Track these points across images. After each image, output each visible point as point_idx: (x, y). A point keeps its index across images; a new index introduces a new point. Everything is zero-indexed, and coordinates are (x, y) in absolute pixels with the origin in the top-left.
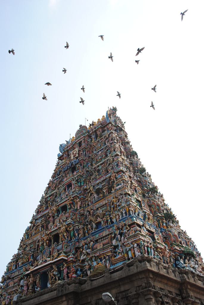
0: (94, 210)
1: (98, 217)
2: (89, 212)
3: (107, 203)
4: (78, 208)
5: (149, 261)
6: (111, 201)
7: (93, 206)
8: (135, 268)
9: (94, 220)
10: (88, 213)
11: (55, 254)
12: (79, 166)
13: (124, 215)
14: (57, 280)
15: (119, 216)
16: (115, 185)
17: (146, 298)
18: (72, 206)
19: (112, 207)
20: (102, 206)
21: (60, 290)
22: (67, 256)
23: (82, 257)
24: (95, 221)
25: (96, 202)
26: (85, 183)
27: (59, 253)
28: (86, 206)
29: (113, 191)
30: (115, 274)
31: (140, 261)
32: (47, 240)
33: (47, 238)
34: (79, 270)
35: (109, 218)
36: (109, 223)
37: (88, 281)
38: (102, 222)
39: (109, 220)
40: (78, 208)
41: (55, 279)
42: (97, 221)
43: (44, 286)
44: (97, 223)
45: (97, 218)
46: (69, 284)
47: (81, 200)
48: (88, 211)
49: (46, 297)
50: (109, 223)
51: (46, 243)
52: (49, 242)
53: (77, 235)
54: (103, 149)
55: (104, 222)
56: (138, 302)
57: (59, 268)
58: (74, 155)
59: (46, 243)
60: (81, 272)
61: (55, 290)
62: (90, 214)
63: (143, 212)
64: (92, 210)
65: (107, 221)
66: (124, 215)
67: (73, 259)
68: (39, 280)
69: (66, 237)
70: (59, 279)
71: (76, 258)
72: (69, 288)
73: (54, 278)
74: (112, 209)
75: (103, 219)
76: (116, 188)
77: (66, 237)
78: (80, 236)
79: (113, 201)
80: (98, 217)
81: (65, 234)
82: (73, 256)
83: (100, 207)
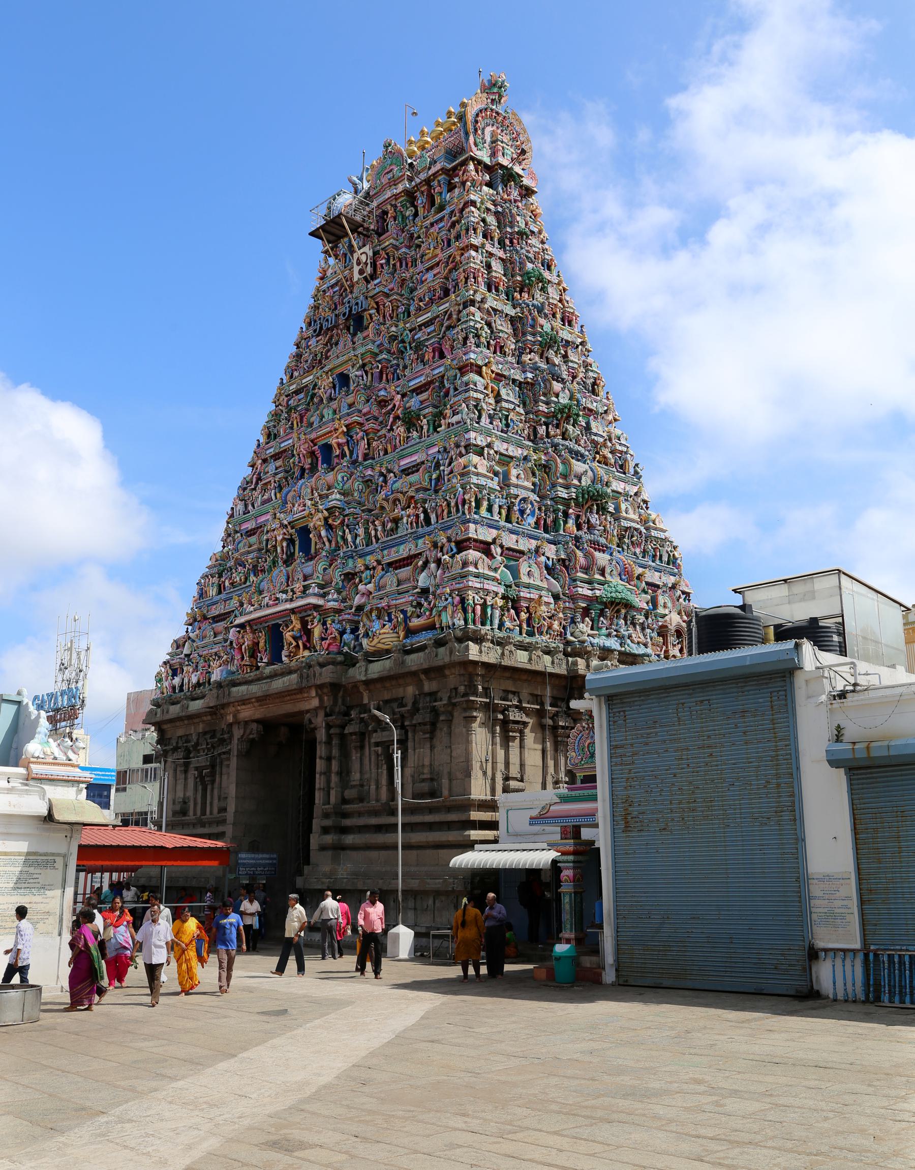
4: (360, 459)
5: (479, 639)
6: (435, 458)
8: (448, 653)
11: (298, 586)
12: (370, 315)
13: (453, 510)
14: (301, 650)
15: (443, 511)
16: (447, 411)
17: (467, 714)
21: (305, 675)
22: (324, 596)
23: (358, 600)
26: (384, 376)
27: (306, 583)
29: (443, 427)
30: (413, 656)
31: (460, 640)
32: (284, 539)
33: (285, 534)
34: (348, 631)
37: (361, 664)
39: (422, 516)
40: (360, 459)
41: (297, 646)
43: (276, 658)
46: (322, 665)
47: (367, 435)
48: (382, 474)
49: (279, 684)
51: (282, 547)
52: (288, 546)
53: (349, 538)
54: (437, 264)
56: (451, 721)
57: (304, 623)
58: (360, 267)
59: (282, 547)
60: (352, 636)
61: (295, 671)
63: (509, 496)
65: (417, 516)
66: (453, 510)
67: (336, 603)
68: (266, 642)
69: (325, 539)
70: (305, 648)
71: (344, 600)
72: (320, 674)
73: (294, 644)
76: (450, 421)
77: (325, 539)
78: (358, 541)
81: (323, 533)
82: (335, 596)
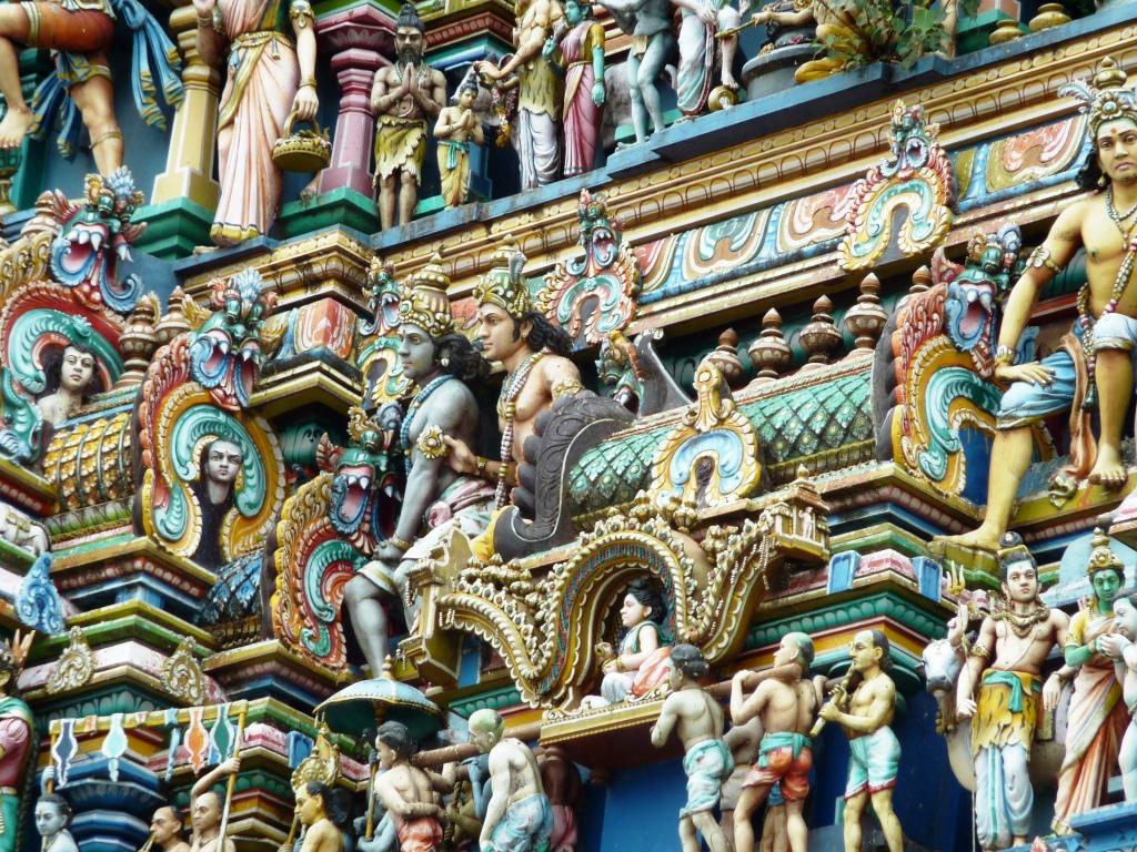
0: (586, 363)
1: (632, 608)
2: (484, 385)
3: (924, 257)
6: (1033, 235)
7: (599, 229)
9: (522, 668)
10: (446, 396)
18: (95, 105)
19: (1023, 395)
20: (795, 308)
24: (548, 688)
25: (670, 157)
28: (429, 182)
35: (878, 687)
36: (868, 818)
38: (703, 761)
39: (878, 756)
42: (591, 715)
44: (574, 751)
45: (613, 630)
50: (868, 818)
55: (742, 750)
62: (478, 424)
64: (540, 335)
74: (1009, 455)
75: (739, 706)
79: (1076, 241)
80: (632, 608)
83: (746, 322)
